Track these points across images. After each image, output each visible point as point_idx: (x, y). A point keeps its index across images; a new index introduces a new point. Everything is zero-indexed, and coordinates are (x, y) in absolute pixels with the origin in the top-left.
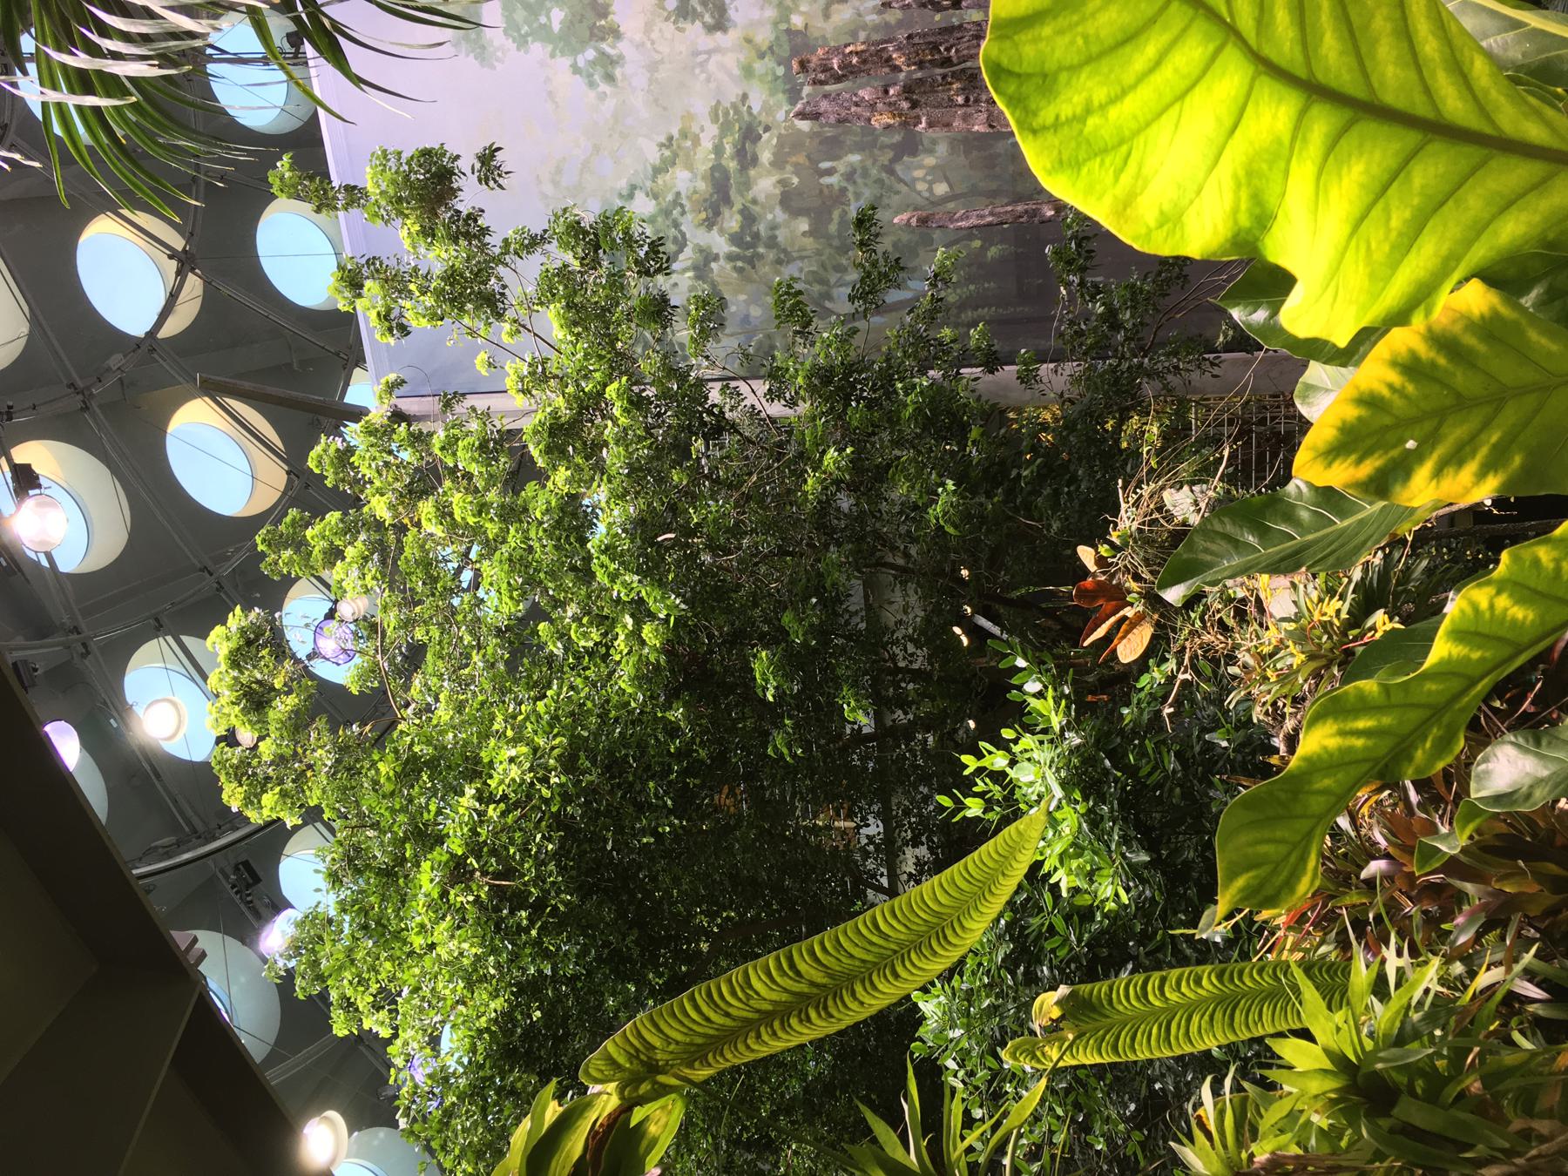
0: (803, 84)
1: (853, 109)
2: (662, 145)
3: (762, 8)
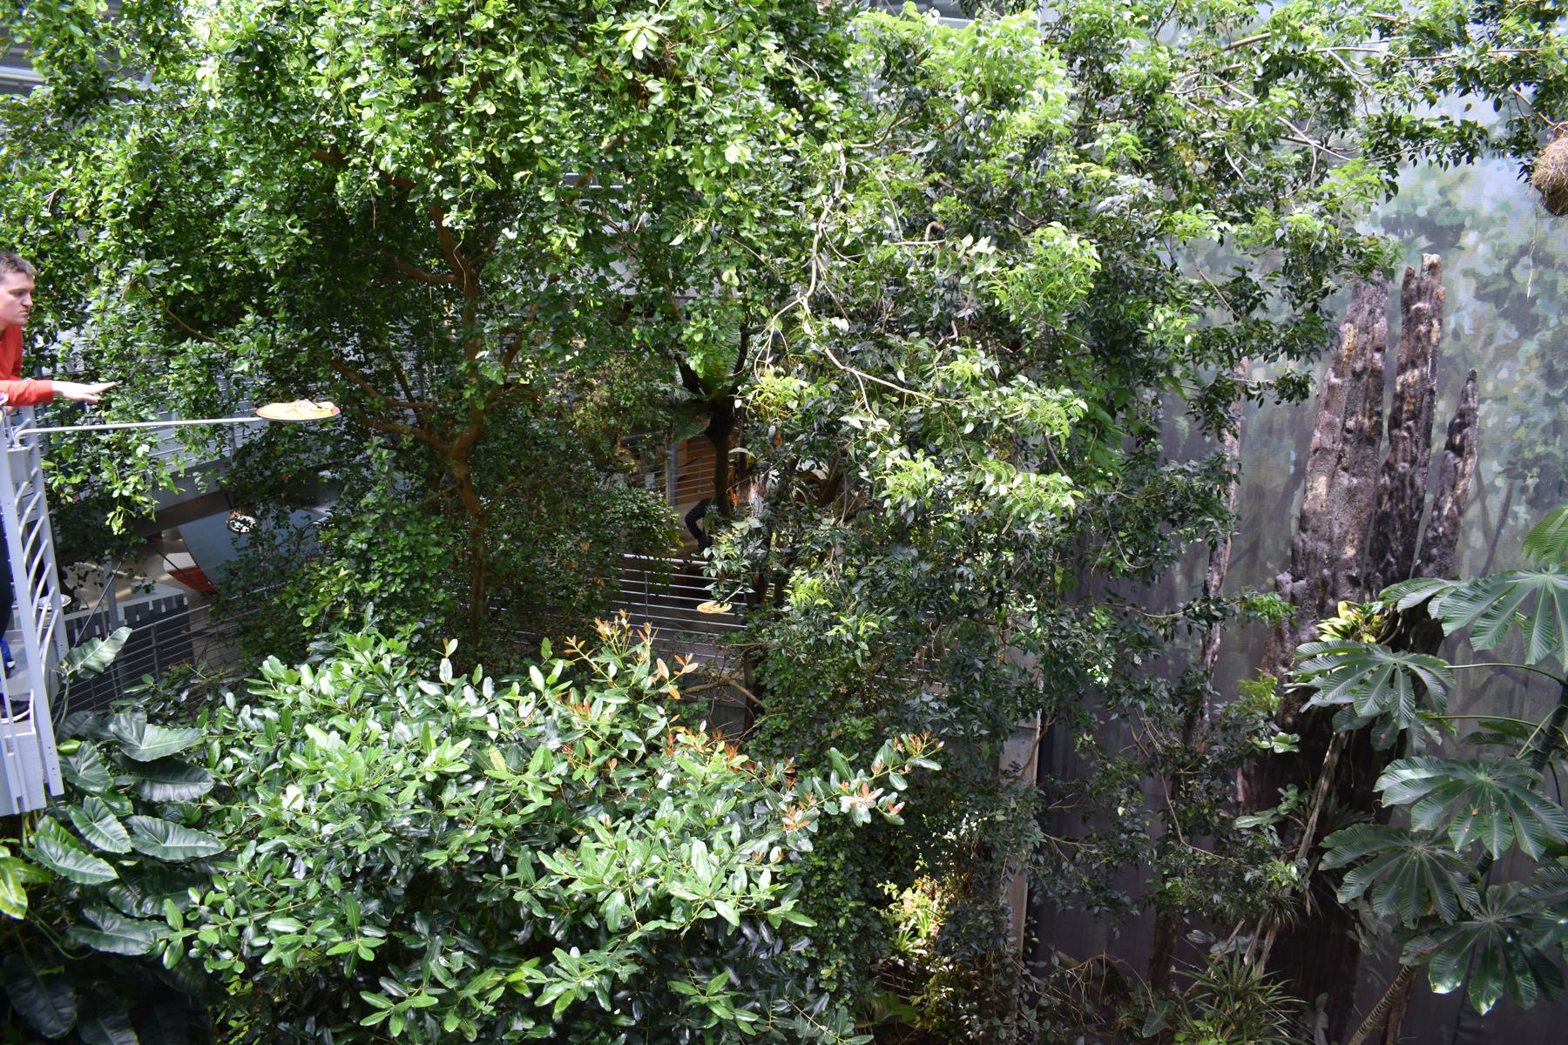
0: (1401, 236)
1: (1367, 307)
3: (1493, 199)
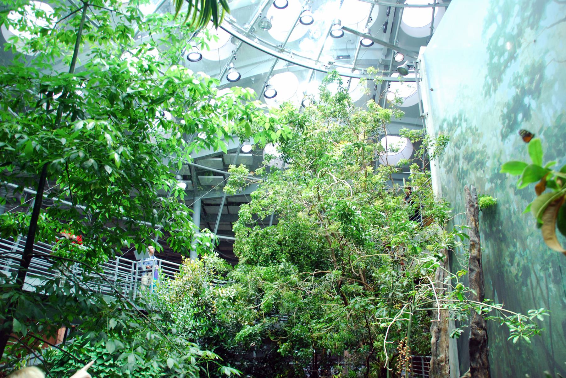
2: (475, 127)
